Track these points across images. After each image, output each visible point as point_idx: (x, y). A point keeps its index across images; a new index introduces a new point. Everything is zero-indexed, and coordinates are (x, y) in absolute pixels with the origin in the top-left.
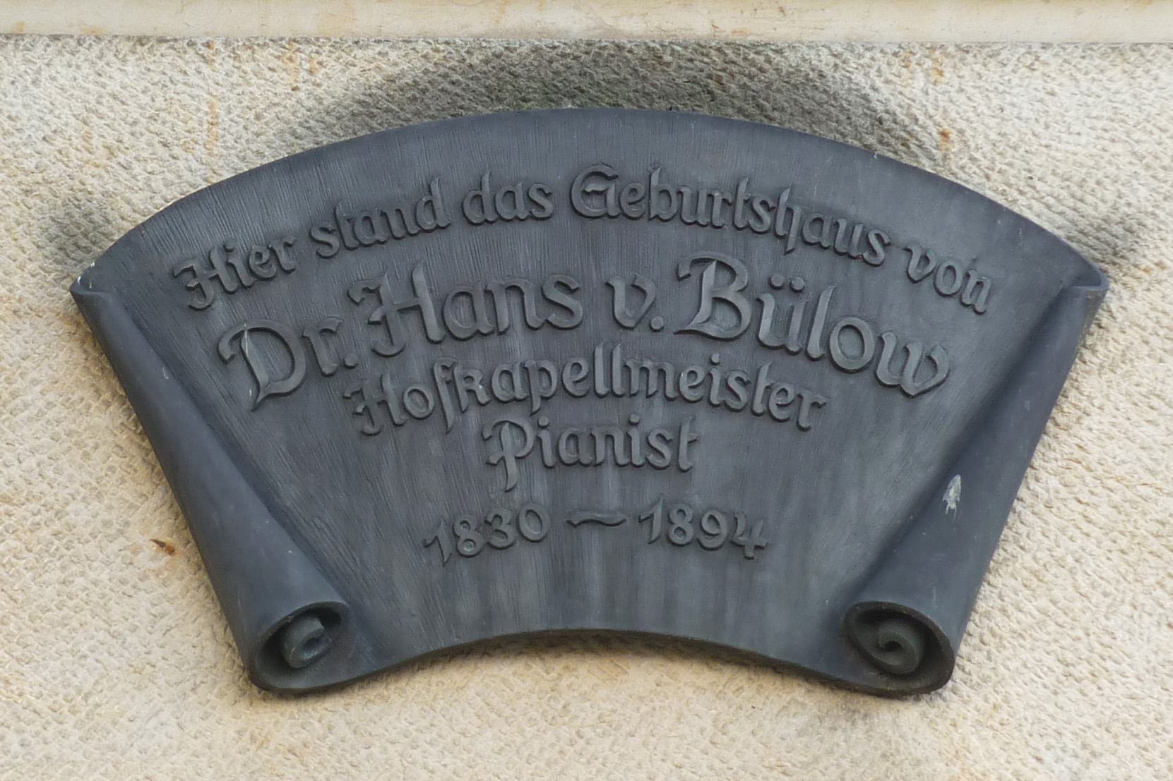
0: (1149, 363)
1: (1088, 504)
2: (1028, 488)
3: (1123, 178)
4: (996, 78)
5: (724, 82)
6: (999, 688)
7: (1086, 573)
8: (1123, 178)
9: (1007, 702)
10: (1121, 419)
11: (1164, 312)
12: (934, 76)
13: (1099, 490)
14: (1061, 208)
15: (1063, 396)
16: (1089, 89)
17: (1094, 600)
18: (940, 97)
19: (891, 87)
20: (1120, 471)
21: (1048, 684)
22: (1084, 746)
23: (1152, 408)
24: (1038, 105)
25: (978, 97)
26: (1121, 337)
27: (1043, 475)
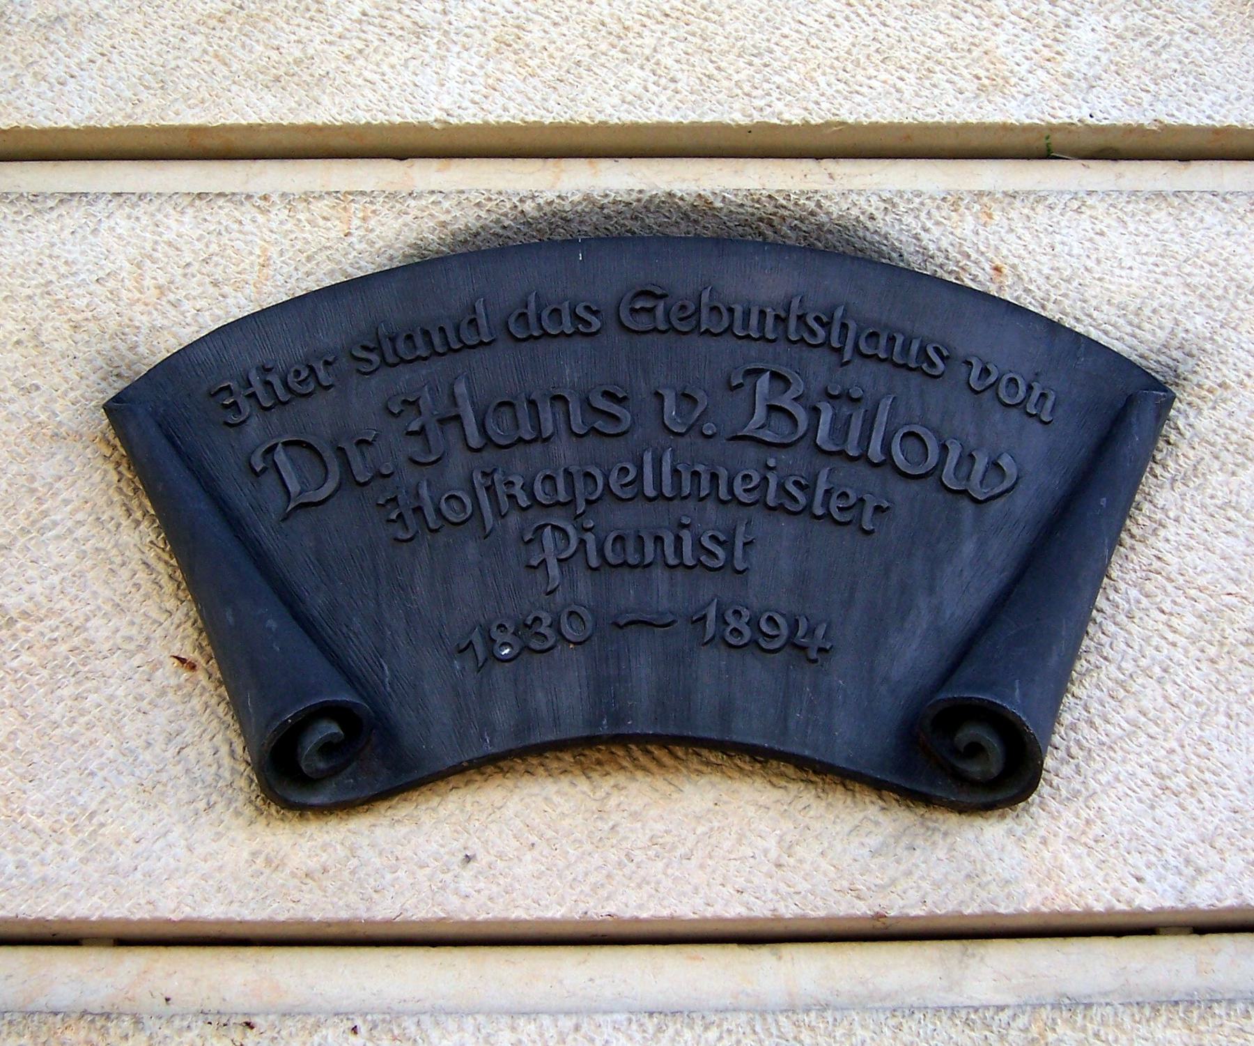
0: (1221, 477)
1: (1171, 614)
2: (1108, 599)
3: (1178, 306)
4: (1046, 221)
5: (775, 223)
6: (1091, 803)
7: (1176, 683)
8: (1178, 306)
9: (1101, 818)
10: (1197, 531)
11: (1232, 429)
12: (984, 218)
13: (1181, 600)
14: (1119, 334)
15: (1137, 508)
16: (1137, 229)
17: (1186, 710)
18: (990, 237)
19: (941, 228)
20: (1201, 581)
21: (1144, 798)
22: (1188, 862)
23: (1229, 520)
24: (1088, 244)
25: (1027, 236)
26: (1191, 453)
27: (1122, 586)
